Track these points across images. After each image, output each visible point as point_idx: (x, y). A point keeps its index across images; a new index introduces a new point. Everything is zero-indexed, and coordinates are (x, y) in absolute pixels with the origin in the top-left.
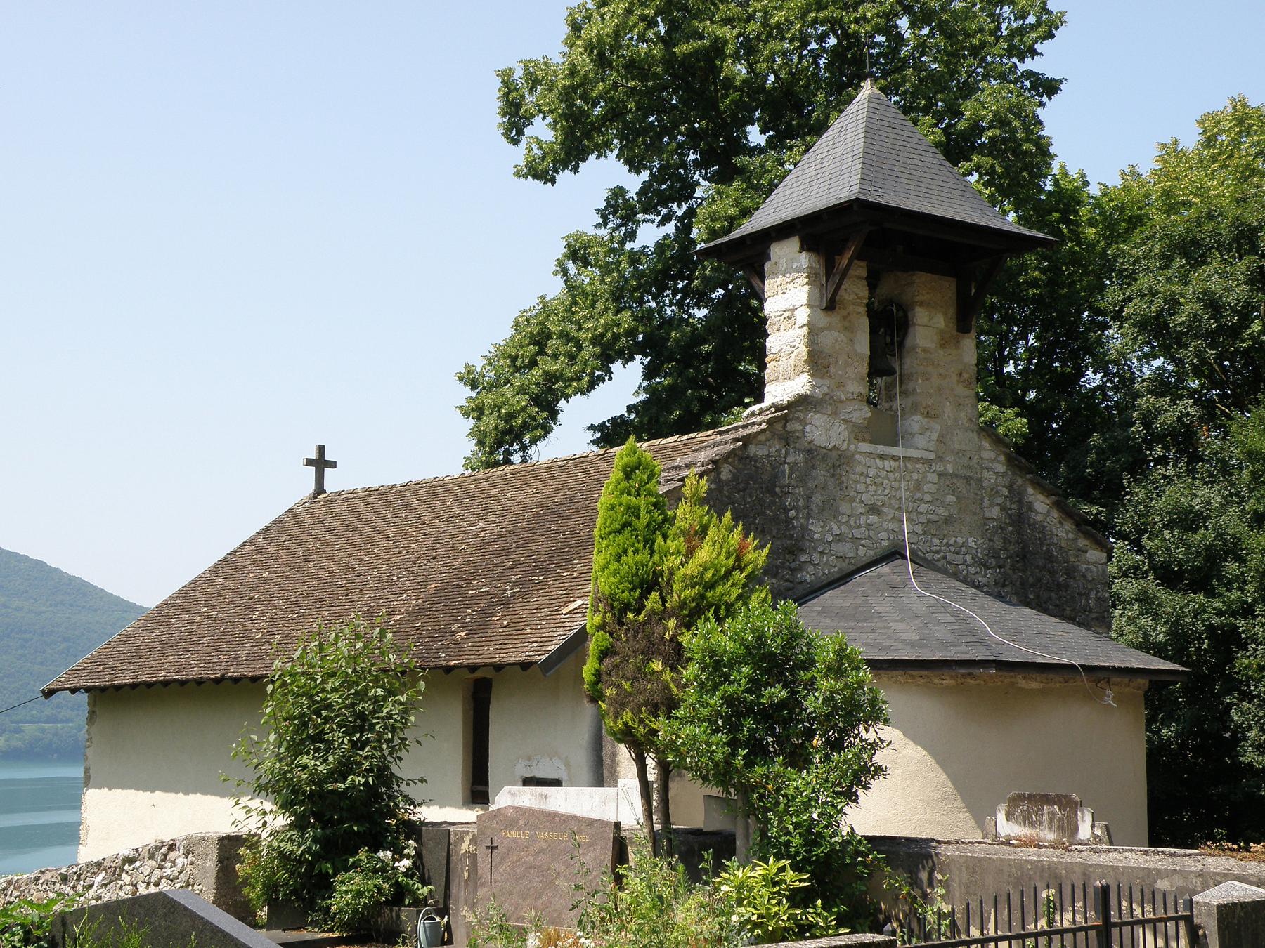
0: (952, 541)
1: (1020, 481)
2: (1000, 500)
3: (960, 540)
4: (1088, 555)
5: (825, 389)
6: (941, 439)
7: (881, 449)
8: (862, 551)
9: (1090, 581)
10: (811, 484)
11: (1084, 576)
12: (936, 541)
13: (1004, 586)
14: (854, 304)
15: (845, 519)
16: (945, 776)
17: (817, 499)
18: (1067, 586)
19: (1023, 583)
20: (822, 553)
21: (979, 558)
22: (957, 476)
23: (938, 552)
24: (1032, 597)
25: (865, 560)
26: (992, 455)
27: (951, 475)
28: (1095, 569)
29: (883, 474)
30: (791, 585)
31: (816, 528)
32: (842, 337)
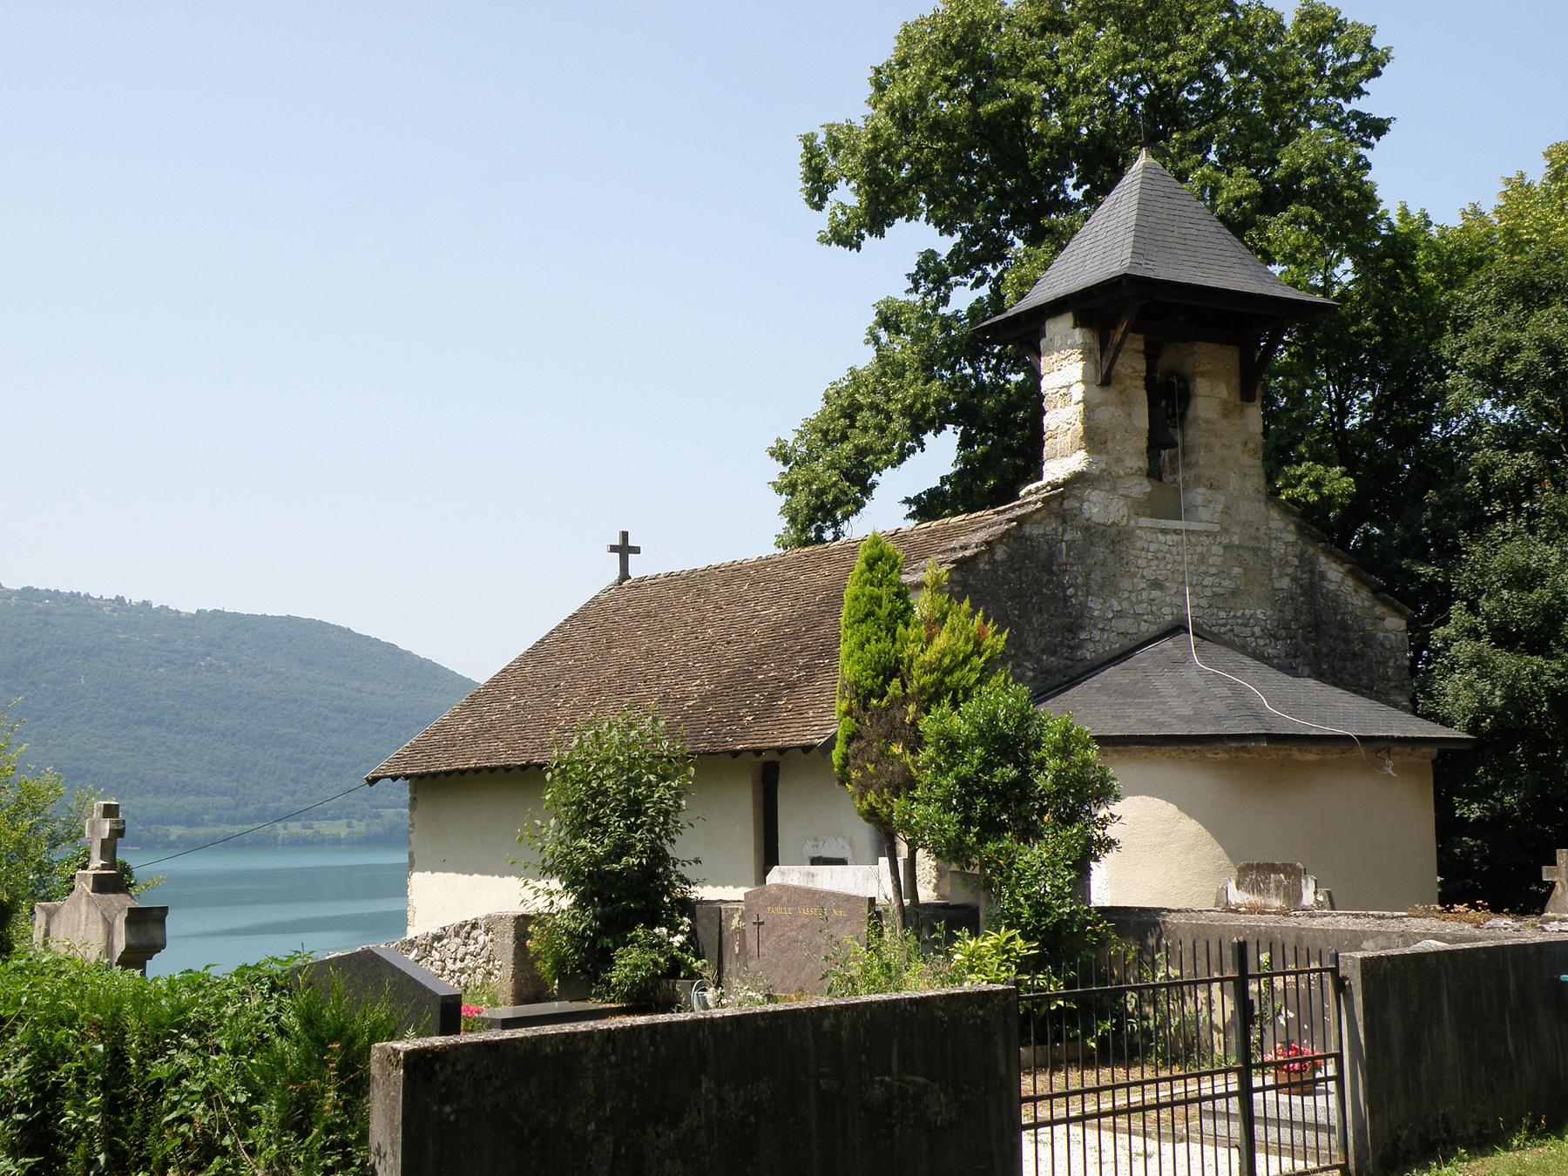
0: (1239, 614)
1: (1311, 550)
2: (1290, 570)
3: (1248, 613)
4: (1386, 623)
5: (1103, 465)
6: (1226, 511)
7: (1163, 523)
8: (1144, 627)
9: (1389, 650)
10: (1090, 561)
11: (1382, 645)
12: (1222, 614)
13: (1296, 657)
14: (1131, 378)
15: (1126, 595)
16: (1221, 849)
17: (1096, 576)
18: (1363, 655)
19: (1316, 653)
20: (1102, 630)
21: (1268, 630)
22: (1243, 547)
23: (1224, 625)
24: (1325, 667)
25: (1147, 636)
26: (1281, 525)
27: (1237, 547)
28: (1393, 637)
29: (1165, 548)
30: (1070, 663)
31: (1095, 606)
32: (1119, 411)
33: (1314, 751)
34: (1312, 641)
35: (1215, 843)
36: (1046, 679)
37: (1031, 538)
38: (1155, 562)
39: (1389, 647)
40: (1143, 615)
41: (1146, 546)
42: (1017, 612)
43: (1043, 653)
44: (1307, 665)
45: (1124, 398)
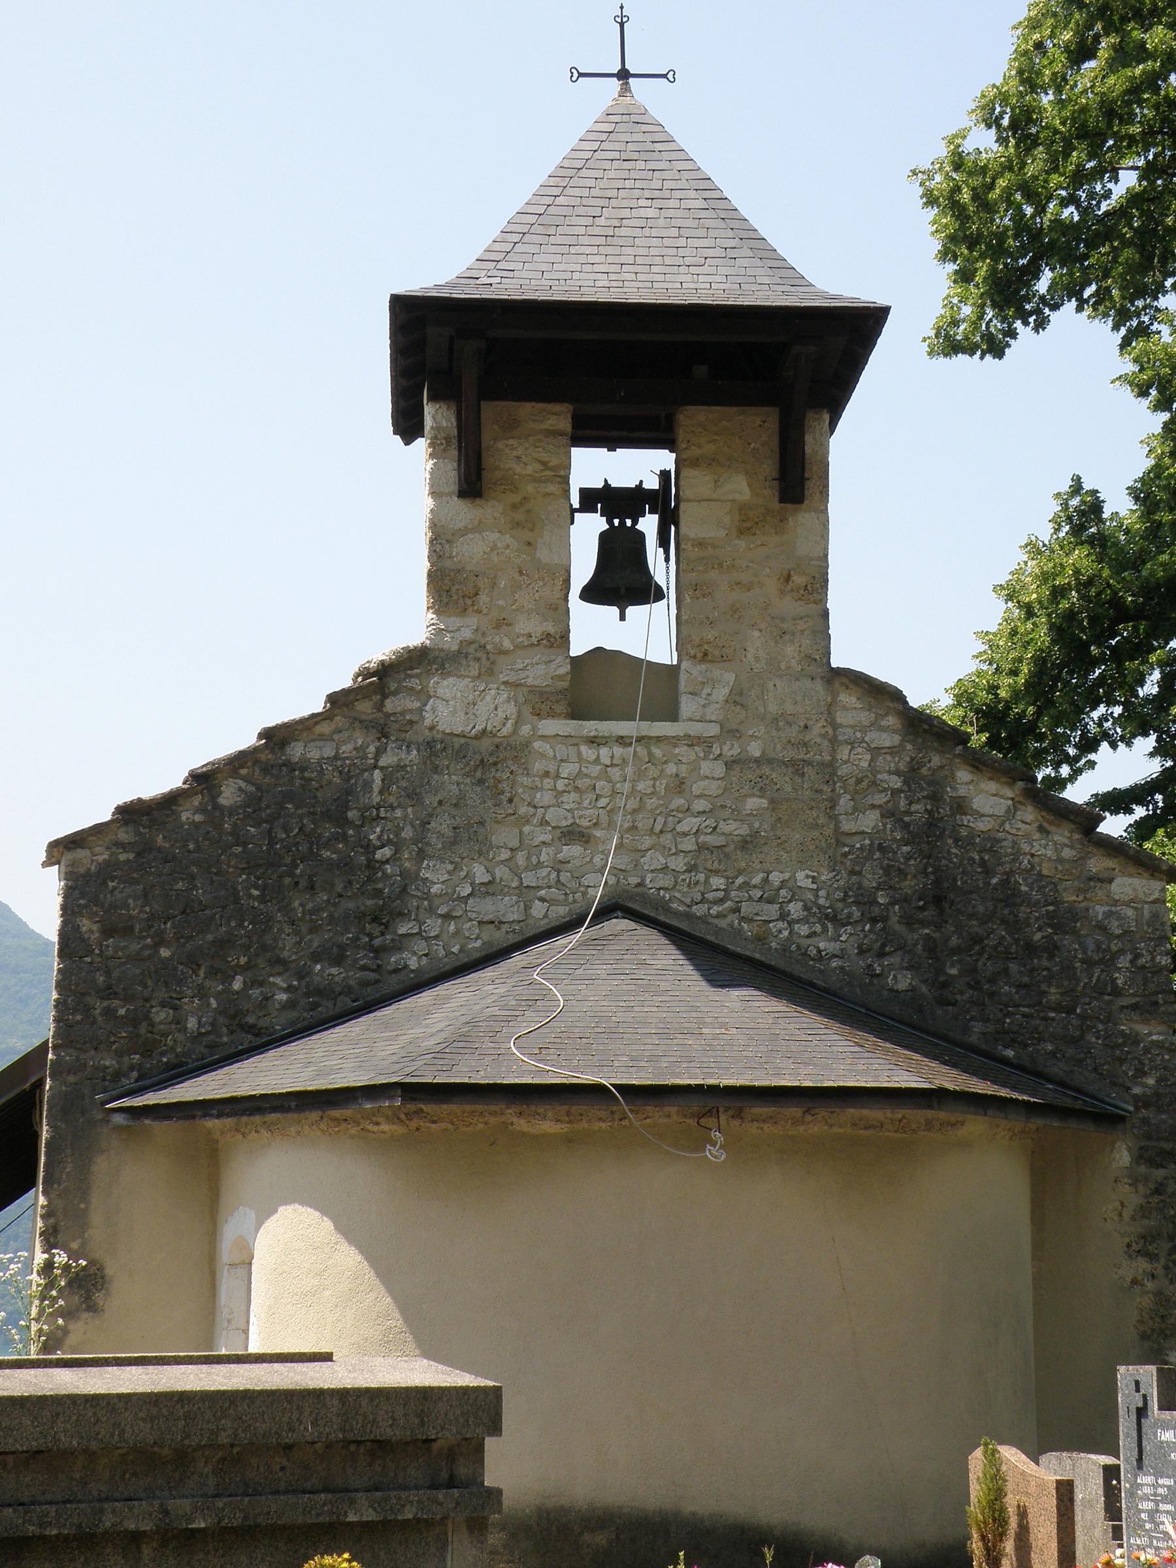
0: (757, 880)
1: (936, 760)
2: (880, 799)
3: (776, 878)
4: (1114, 885)
5: (467, 634)
6: (737, 698)
7: (591, 727)
8: (538, 909)
9: (1118, 937)
10: (430, 800)
11: (1102, 928)
12: (718, 882)
13: (881, 954)
14: (536, 480)
15: (505, 855)
16: (389, 1300)
17: (442, 825)
18: (1052, 949)
19: (932, 948)
20: (447, 917)
21: (819, 907)
22: (770, 761)
23: (721, 901)
24: (954, 971)
25: (544, 925)
26: (865, 717)
27: (757, 761)
28: (1130, 913)
29: (596, 770)
30: (372, 976)
31: (436, 876)
32: (508, 539)
33: (550, 1114)
34: (923, 923)
35: (383, 1291)
36: (314, 1007)
37: (303, 766)
38: (573, 796)
39: (1118, 932)
40: (539, 888)
41: (552, 768)
42: (256, 893)
43: (316, 962)
44: (908, 969)
45: (520, 516)
